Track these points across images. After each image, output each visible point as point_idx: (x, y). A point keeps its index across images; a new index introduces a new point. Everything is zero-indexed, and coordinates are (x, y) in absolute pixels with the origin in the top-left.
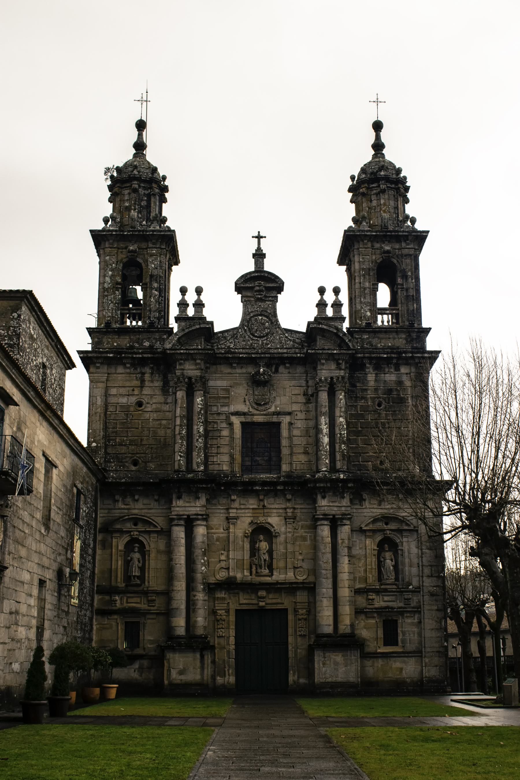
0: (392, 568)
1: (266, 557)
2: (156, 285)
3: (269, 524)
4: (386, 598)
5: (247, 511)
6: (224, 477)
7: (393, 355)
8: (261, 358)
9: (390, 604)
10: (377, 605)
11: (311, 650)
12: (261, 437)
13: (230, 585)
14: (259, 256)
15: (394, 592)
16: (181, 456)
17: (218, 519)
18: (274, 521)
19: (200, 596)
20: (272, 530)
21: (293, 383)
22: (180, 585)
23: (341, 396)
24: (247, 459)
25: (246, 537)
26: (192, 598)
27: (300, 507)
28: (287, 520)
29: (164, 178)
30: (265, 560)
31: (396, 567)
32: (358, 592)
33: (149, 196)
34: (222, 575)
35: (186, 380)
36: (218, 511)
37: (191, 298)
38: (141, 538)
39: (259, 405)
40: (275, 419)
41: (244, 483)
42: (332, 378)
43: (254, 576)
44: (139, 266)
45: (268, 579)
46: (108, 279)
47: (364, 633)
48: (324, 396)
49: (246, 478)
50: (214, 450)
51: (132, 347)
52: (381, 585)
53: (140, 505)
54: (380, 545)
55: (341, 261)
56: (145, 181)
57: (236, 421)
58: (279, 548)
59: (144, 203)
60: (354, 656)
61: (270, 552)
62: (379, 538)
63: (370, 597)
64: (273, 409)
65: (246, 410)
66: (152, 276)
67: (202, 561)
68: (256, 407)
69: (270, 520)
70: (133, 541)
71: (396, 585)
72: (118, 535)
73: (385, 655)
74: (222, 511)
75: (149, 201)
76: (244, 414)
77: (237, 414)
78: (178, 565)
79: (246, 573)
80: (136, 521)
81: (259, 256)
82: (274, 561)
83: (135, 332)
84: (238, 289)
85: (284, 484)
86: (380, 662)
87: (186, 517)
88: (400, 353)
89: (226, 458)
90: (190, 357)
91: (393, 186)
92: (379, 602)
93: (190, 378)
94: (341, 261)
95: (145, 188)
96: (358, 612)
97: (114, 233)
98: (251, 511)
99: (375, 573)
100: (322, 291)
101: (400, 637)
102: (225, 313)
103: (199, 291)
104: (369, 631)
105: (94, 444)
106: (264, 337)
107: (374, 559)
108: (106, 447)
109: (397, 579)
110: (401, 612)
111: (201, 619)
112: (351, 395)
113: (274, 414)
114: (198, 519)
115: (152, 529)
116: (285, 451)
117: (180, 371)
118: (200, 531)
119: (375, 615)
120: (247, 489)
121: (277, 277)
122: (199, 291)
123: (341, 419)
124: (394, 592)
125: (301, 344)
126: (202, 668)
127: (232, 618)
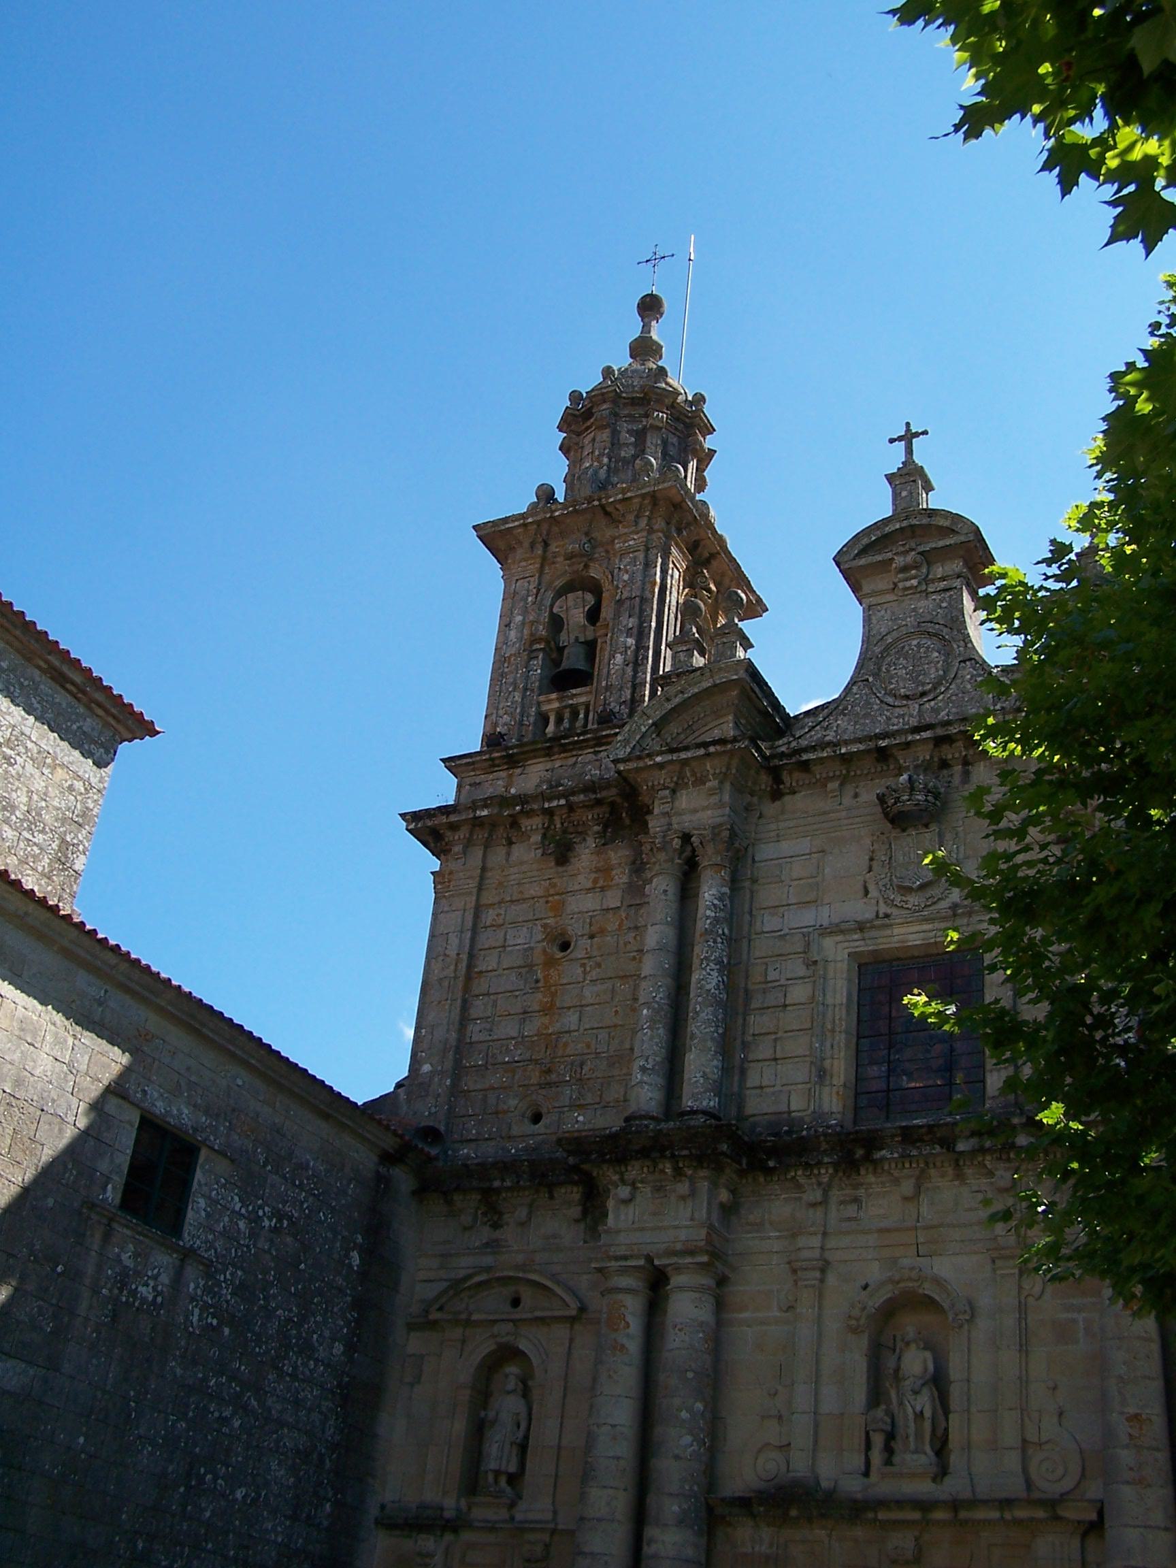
1: (925, 1402)
3: (937, 1281)
6: (789, 1133)
8: (908, 745)
14: (908, 479)
16: (643, 1069)
18: (957, 1268)
24: (874, 1071)
25: (855, 1330)
28: (999, 1263)
29: (700, 399)
30: (920, 1416)
33: (641, 435)
35: (677, 843)
38: (523, 1345)
39: (909, 890)
44: (596, 589)
46: (513, 635)
50: (763, 1050)
56: (633, 402)
57: (837, 954)
61: (938, 1381)
65: (869, 915)
66: (620, 602)
67: (684, 1415)
69: (943, 1267)
70: (507, 1354)
72: (457, 1333)
76: (861, 927)
77: (835, 929)
78: (604, 1429)
81: (908, 479)
82: (955, 1421)
83: (564, 749)
84: (853, 578)
87: (642, 1262)
89: (800, 1073)
93: (686, 838)
95: (632, 418)
97: (530, 520)
102: (808, 650)
105: (426, 1068)
106: (923, 694)
108: (458, 1071)
114: (678, 1269)
117: (664, 821)
118: (687, 1307)
121: (958, 518)
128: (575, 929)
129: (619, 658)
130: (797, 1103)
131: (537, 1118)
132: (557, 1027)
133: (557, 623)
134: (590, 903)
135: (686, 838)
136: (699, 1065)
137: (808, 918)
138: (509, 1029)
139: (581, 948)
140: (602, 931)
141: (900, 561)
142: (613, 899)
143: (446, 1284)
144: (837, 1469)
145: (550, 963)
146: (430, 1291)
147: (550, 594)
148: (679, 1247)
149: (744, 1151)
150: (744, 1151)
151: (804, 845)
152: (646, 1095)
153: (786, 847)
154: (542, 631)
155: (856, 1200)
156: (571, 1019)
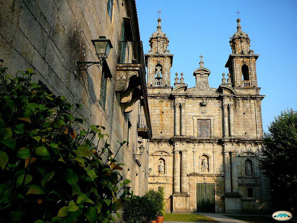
0: (250, 170)
1: (207, 165)
2: (167, 73)
3: (208, 154)
4: (249, 180)
5: (200, 149)
7: (249, 97)
9: (250, 182)
10: (245, 183)
11: (223, 198)
12: (204, 123)
13: (194, 174)
15: (251, 178)
17: (190, 152)
19: (185, 178)
20: (208, 156)
21: (214, 106)
22: (178, 174)
23: (232, 110)
26: (182, 179)
27: (219, 148)
31: (252, 169)
32: (239, 178)
34: (191, 171)
36: (190, 149)
37: (179, 77)
40: (209, 118)
41: (199, 140)
42: (228, 104)
43: (203, 172)
44: (161, 66)
45: (208, 173)
47: (241, 193)
48: (226, 111)
49: (199, 138)
51: (159, 93)
52: (247, 176)
53: (163, 147)
54: (246, 161)
55: (226, 66)
57: (195, 119)
58: (211, 161)
59: (162, 46)
60: (238, 200)
62: (245, 159)
63: (243, 180)
64: (208, 115)
65: (199, 115)
68: (202, 113)
69: (208, 152)
71: (252, 176)
73: (248, 200)
74: (191, 149)
75: (163, 44)
79: (200, 170)
80: (162, 152)
85: (212, 140)
86: (247, 203)
88: (251, 96)
90: (180, 96)
91: (246, 40)
92: (247, 182)
94: (226, 66)
95: (162, 41)
96: (240, 185)
98: (201, 149)
99: (245, 172)
100: (223, 75)
101: (254, 194)
103: (182, 74)
104: (242, 192)
107: (244, 167)
109: (252, 174)
110: (254, 185)
111: (185, 186)
112: (235, 110)
113: (208, 116)
115: (168, 155)
116: (212, 129)
118: (184, 156)
119: (245, 186)
120: (200, 141)
121: (208, 70)
122: (182, 74)
123: (232, 118)
124: (251, 178)
125: (217, 92)
126: (186, 203)
127: (196, 186)
128: (164, 111)
129: (166, 77)
130: (192, 135)
131: (161, 133)
132: (163, 123)
133: (156, 70)
134: (165, 108)
135: (180, 104)
136: (183, 130)
137: (193, 114)
138: (157, 122)
139: (165, 113)
140: (168, 112)
141: (202, 74)
142: (169, 108)
143: (154, 151)
144: (197, 171)
145: (161, 115)
146: (152, 152)
147: (155, 66)
148: (183, 150)
149: (190, 140)
150: (190, 140)
151: (191, 106)
152: (178, 133)
153: (189, 106)
154: (155, 71)
155: (199, 145)
156: (165, 122)
